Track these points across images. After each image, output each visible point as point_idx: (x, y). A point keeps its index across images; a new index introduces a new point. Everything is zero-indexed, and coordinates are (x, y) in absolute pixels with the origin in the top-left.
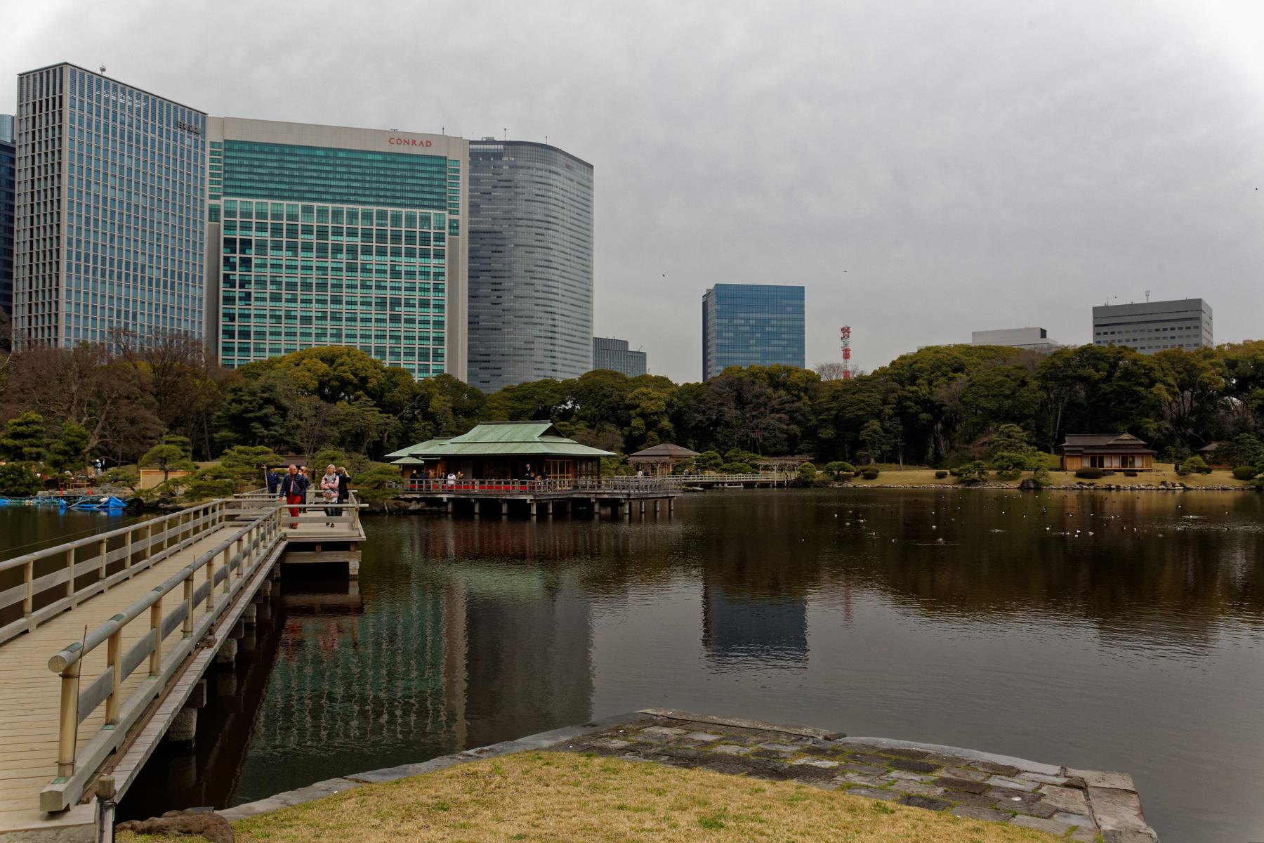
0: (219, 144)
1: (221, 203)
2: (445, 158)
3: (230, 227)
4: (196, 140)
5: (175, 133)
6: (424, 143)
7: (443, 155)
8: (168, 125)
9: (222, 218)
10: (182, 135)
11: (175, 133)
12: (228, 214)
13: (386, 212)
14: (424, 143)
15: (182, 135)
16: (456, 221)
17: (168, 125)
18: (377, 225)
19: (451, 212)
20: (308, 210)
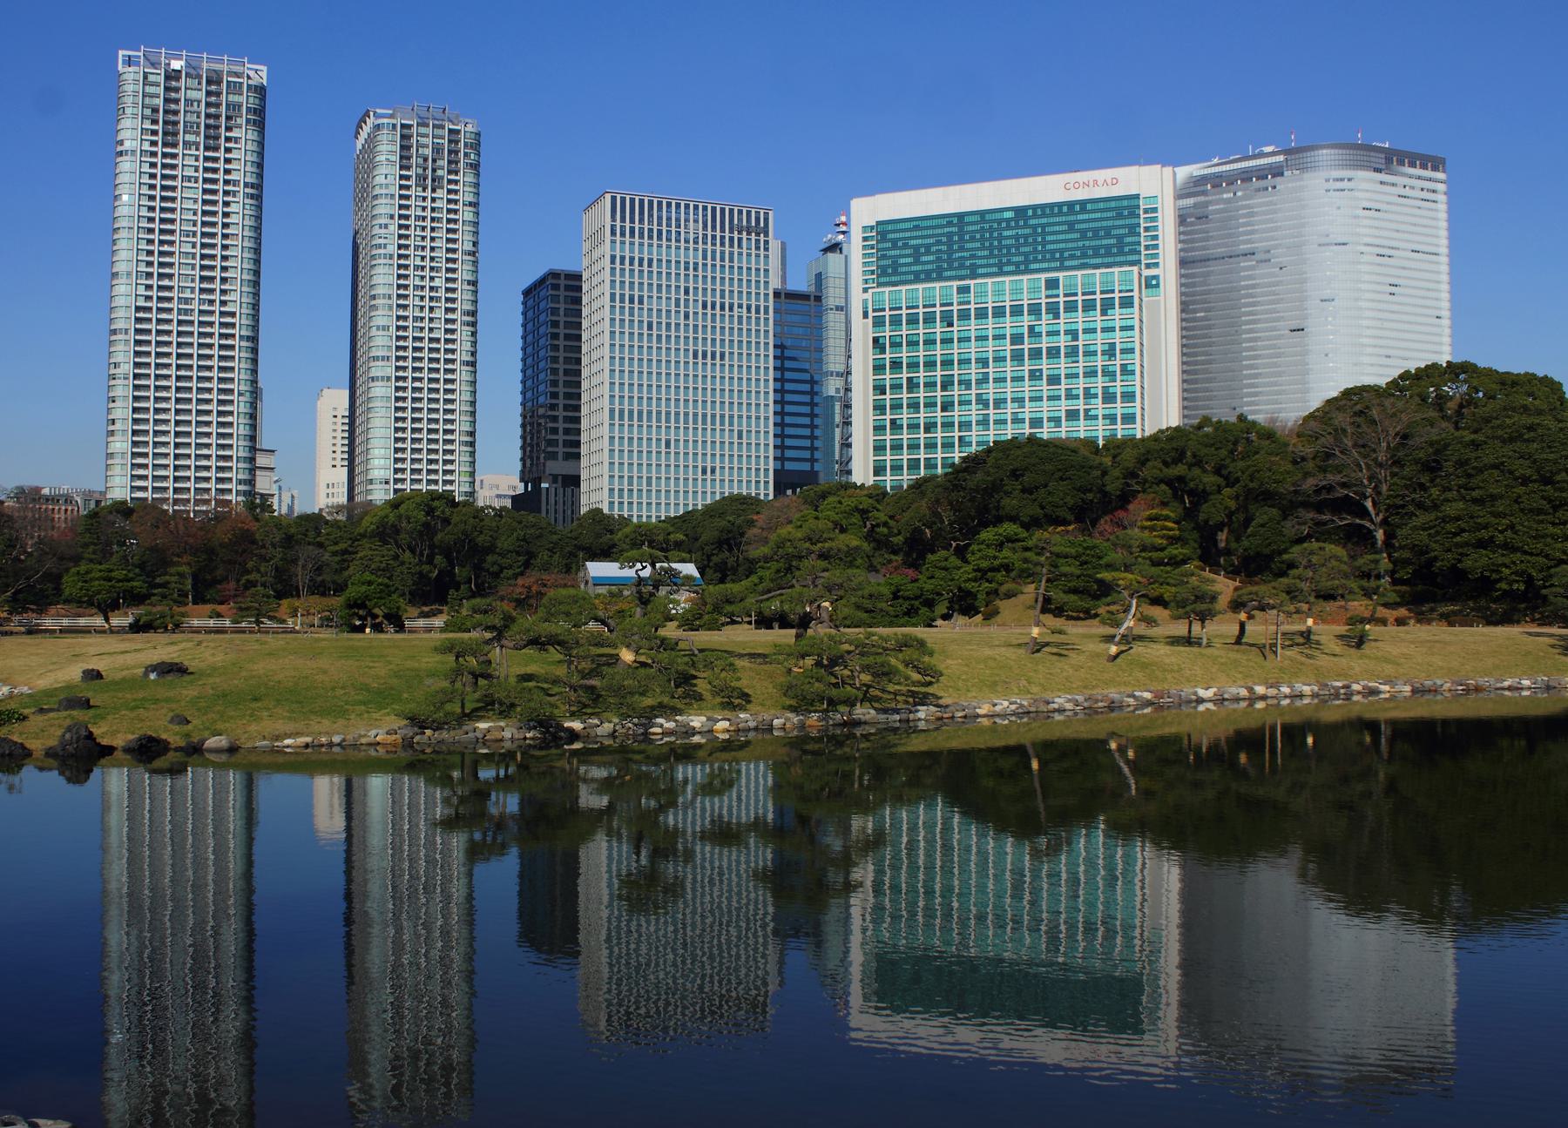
0: (872, 227)
1: (868, 296)
2: (1137, 197)
3: (878, 322)
4: (758, 241)
5: (731, 239)
6: (1109, 182)
7: (1134, 192)
8: (723, 230)
9: (871, 314)
10: (740, 240)
11: (731, 239)
12: (874, 311)
13: (1057, 280)
14: (1109, 182)
15: (740, 240)
16: (1156, 277)
17: (723, 230)
18: (1047, 297)
19: (1148, 266)
20: (964, 290)
